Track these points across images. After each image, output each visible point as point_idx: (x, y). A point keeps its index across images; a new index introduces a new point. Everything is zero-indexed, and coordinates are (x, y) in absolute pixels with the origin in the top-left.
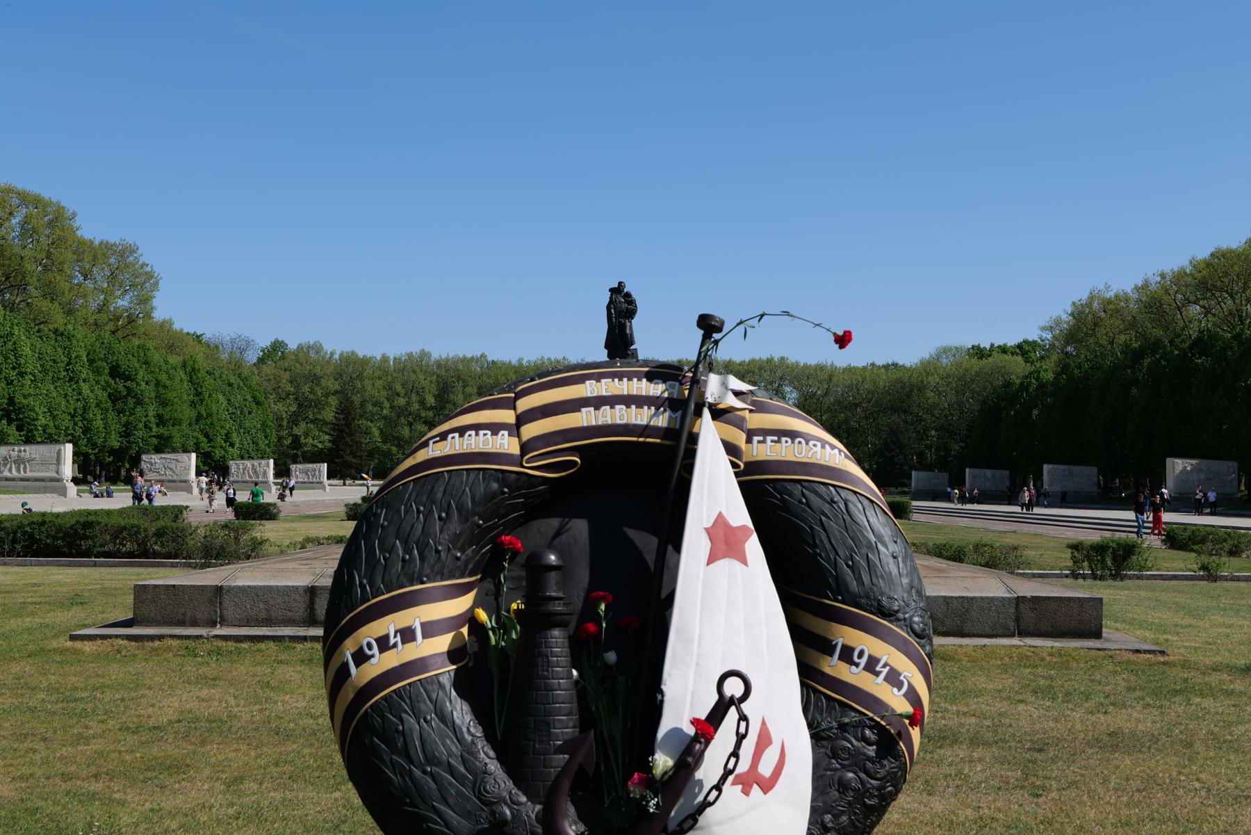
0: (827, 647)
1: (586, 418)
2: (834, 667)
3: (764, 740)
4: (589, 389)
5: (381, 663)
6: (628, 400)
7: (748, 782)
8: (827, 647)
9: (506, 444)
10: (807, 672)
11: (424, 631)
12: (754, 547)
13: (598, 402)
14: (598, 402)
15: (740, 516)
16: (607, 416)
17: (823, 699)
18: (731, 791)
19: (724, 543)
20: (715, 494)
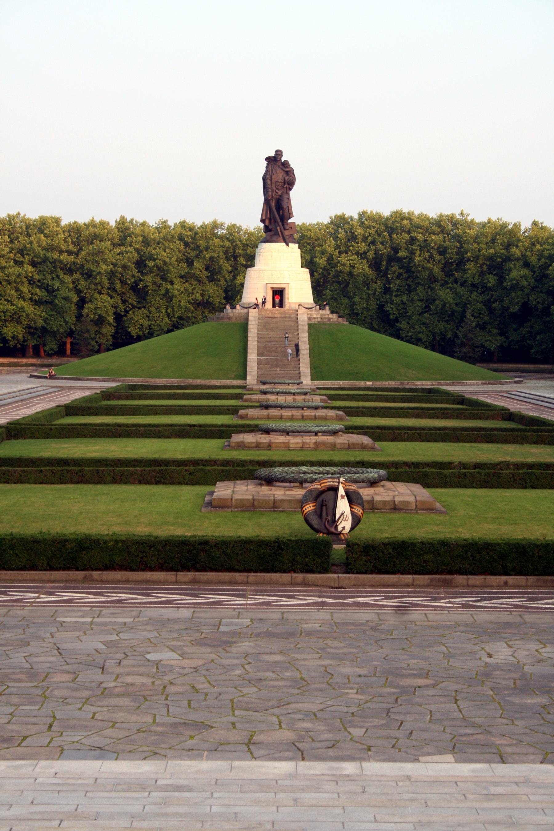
0: (353, 508)
1: (328, 484)
2: (353, 510)
3: (347, 516)
4: (328, 480)
5: (308, 510)
6: (332, 482)
7: (345, 520)
8: (353, 508)
9: (319, 487)
10: (351, 511)
11: (309, 508)
12: (346, 497)
13: (329, 482)
14: (329, 482)
15: (344, 494)
16: (330, 484)
17: (352, 513)
18: (343, 521)
19: (342, 497)
20: (341, 492)
